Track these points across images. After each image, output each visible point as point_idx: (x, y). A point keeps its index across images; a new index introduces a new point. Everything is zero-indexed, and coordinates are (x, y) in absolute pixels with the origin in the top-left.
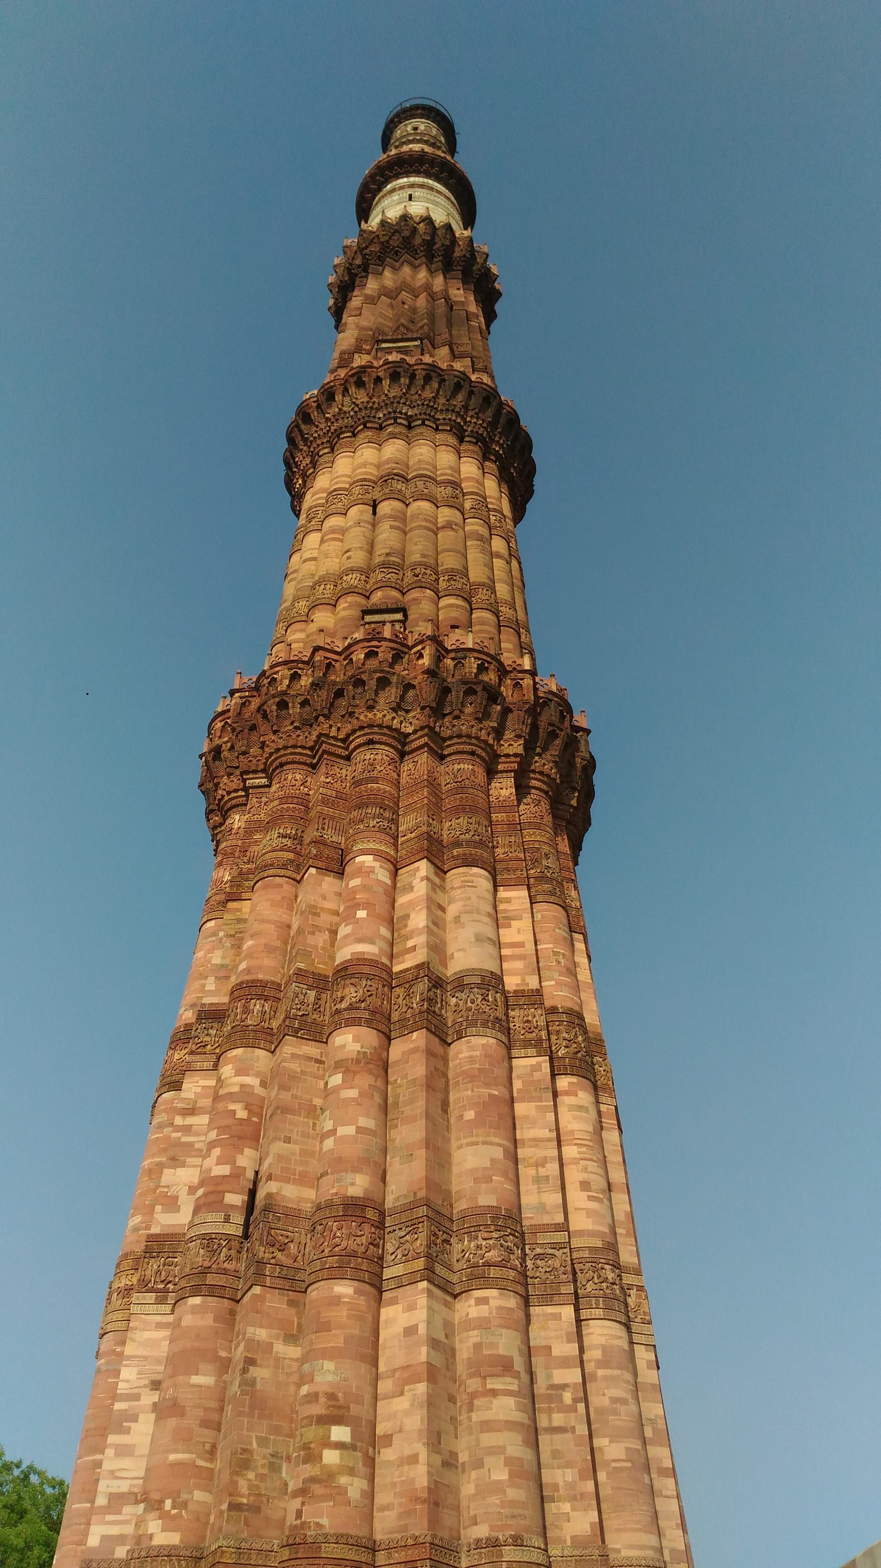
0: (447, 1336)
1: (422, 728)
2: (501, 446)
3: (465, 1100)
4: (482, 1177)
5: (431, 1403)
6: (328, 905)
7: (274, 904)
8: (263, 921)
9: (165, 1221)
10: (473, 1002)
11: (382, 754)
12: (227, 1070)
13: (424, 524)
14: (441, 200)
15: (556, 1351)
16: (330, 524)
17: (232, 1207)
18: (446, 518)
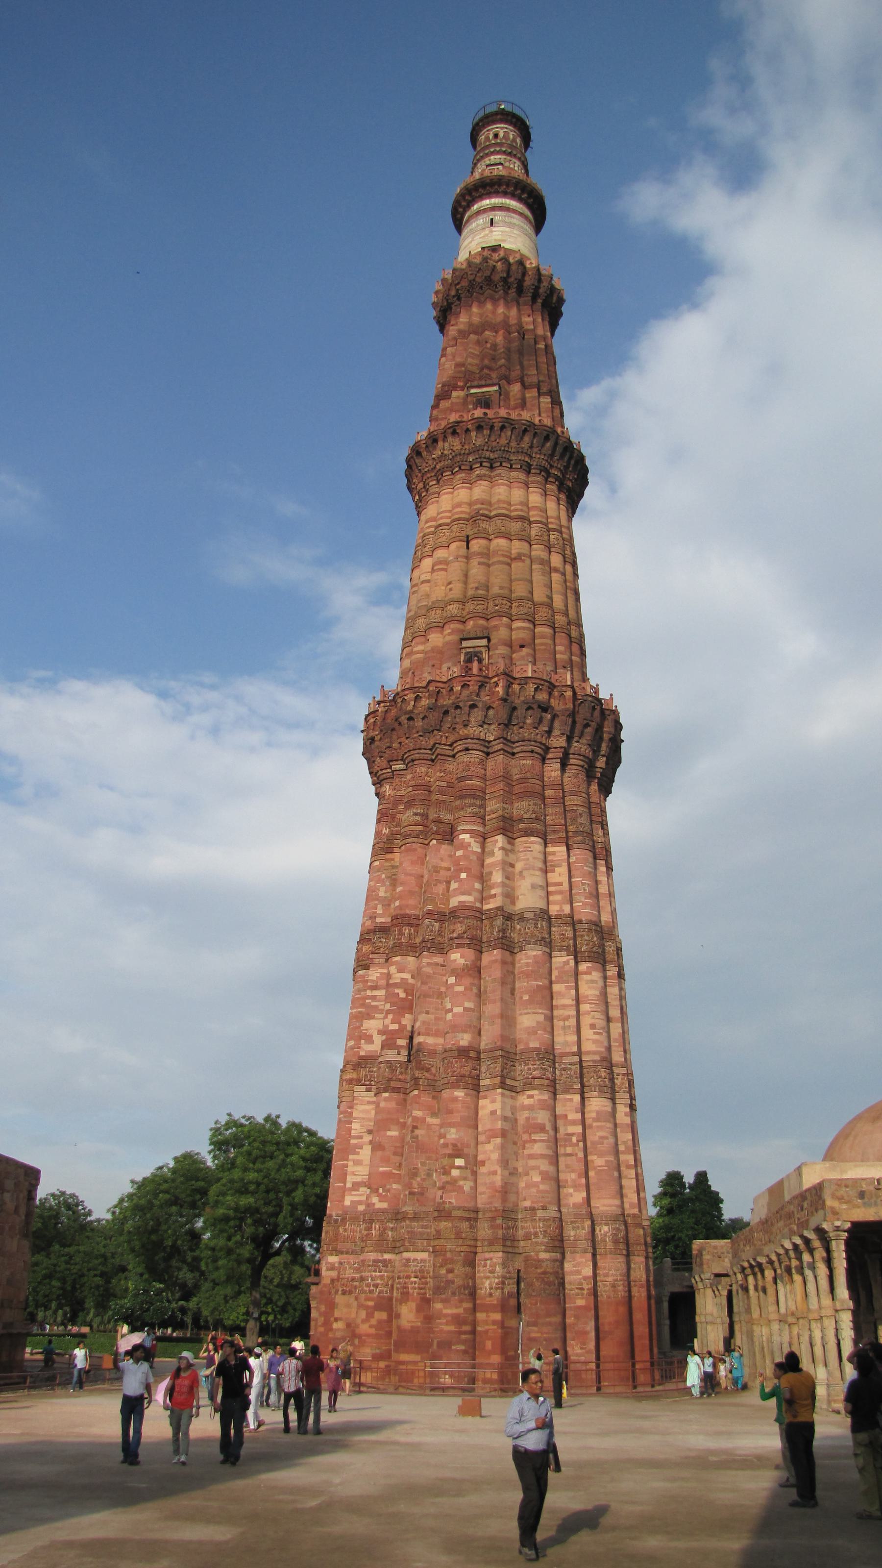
0: (512, 1114)
1: (499, 738)
4: (532, 1032)
5: (503, 1147)
6: (444, 864)
7: (413, 863)
8: (406, 874)
9: (366, 1049)
10: (529, 928)
12: (393, 969)
13: (502, 559)
14: (516, 220)
15: (570, 1117)
16: (439, 555)
17: (402, 1047)
18: (517, 551)
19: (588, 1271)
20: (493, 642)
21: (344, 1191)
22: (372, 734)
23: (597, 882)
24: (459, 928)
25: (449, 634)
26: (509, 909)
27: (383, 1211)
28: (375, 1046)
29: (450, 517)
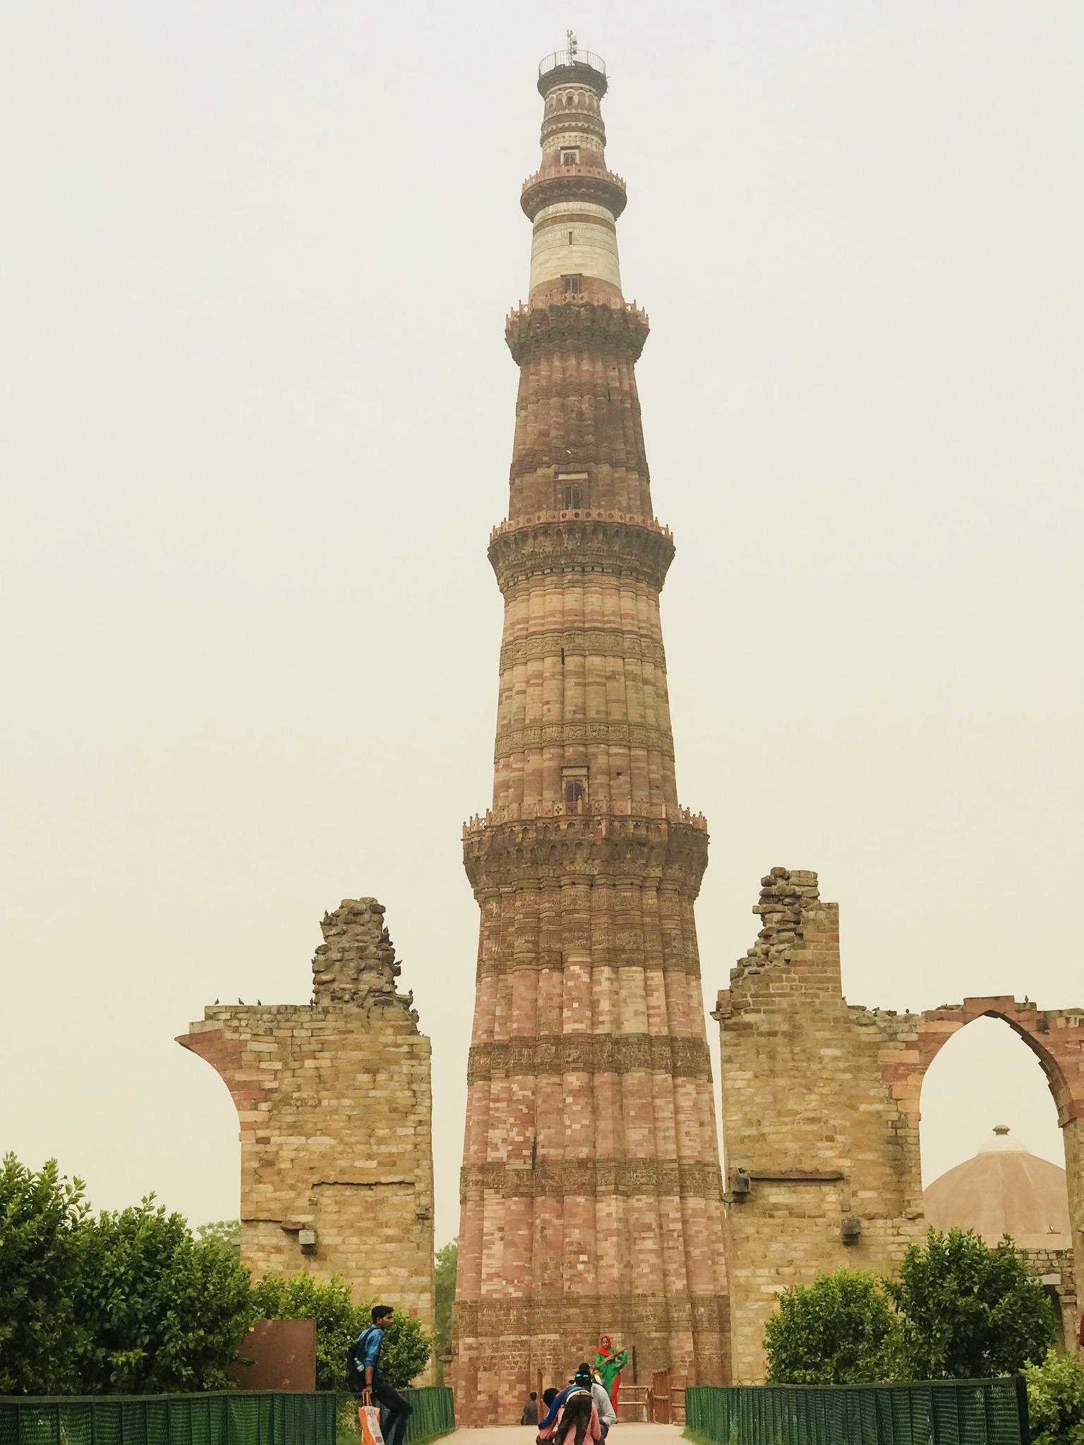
2: (650, 567)
3: (632, 1103)
6: (558, 991)
8: (523, 999)
9: (492, 1156)
11: (581, 888)
12: (515, 1087)
13: (598, 680)
14: (597, 231)
19: (689, 1347)
20: (593, 770)
21: (478, 1281)
22: (476, 853)
23: (690, 997)
24: (574, 1054)
25: (550, 759)
26: (616, 1034)
27: (518, 1299)
28: (502, 1153)
29: (543, 625)
